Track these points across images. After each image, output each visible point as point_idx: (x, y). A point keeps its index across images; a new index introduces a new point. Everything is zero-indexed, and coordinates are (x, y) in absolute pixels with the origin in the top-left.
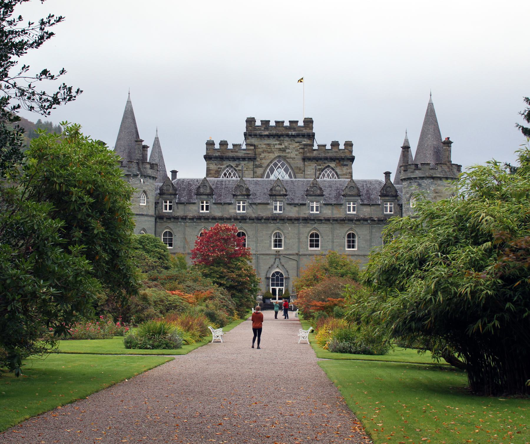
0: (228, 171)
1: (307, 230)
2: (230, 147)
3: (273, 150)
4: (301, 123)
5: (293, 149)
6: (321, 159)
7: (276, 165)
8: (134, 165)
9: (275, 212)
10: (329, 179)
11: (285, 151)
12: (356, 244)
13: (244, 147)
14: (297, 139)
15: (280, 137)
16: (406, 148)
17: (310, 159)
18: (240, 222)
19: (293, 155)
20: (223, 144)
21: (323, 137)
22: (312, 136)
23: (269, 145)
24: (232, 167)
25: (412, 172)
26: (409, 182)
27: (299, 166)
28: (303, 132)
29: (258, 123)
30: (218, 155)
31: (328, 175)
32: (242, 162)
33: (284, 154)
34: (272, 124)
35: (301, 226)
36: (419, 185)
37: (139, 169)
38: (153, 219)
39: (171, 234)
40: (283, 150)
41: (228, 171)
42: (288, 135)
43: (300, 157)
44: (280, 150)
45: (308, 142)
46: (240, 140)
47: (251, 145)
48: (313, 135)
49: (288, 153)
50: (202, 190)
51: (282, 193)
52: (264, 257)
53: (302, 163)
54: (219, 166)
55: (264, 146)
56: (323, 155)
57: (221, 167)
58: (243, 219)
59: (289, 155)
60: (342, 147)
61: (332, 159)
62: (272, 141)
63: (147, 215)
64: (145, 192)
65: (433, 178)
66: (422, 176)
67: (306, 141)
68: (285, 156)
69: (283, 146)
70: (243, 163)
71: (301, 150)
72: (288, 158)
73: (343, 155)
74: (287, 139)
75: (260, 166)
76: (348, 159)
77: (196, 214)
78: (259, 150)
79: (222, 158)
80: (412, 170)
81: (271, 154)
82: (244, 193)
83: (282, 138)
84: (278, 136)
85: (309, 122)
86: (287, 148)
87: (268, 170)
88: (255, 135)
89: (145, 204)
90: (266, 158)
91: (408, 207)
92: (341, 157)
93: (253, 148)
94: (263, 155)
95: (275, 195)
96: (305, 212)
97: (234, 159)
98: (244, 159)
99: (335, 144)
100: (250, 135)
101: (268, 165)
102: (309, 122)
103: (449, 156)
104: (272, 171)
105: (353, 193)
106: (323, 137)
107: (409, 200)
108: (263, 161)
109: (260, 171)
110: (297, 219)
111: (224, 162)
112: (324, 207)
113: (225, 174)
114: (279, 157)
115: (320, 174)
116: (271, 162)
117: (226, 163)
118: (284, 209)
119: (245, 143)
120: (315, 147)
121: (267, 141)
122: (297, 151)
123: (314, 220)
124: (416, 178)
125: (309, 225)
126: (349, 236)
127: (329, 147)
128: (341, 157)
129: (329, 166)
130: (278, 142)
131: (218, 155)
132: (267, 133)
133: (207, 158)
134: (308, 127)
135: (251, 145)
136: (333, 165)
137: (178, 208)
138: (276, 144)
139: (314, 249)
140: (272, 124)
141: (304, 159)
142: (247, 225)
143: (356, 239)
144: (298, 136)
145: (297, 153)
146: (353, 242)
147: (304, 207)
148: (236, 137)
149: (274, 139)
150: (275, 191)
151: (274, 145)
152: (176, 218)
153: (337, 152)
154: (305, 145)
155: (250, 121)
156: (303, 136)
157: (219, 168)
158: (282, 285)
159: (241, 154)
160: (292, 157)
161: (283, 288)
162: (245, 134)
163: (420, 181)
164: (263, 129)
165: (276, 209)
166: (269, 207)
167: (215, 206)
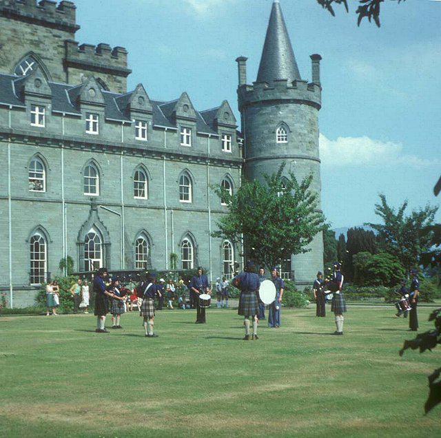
5: (50, 44)
14: (56, 32)
16: (241, 60)
18: (37, 144)
23: (14, 31)
33: (36, 51)
40: (37, 43)
44: (32, 42)
55: (9, 32)
58: (41, 140)
59: (44, 54)
62: (23, 28)
67: (65, 36)
68: (39, 54)
69: (36, 38)
71: (61, 50)
107: (274, 132)
122: (55, 48)
124: (288, 101)
136: (104, 77)
138: (26, 33)
141: (67, 64)
142: (47, 149)
145: (56, 52)
154: (66, 42)
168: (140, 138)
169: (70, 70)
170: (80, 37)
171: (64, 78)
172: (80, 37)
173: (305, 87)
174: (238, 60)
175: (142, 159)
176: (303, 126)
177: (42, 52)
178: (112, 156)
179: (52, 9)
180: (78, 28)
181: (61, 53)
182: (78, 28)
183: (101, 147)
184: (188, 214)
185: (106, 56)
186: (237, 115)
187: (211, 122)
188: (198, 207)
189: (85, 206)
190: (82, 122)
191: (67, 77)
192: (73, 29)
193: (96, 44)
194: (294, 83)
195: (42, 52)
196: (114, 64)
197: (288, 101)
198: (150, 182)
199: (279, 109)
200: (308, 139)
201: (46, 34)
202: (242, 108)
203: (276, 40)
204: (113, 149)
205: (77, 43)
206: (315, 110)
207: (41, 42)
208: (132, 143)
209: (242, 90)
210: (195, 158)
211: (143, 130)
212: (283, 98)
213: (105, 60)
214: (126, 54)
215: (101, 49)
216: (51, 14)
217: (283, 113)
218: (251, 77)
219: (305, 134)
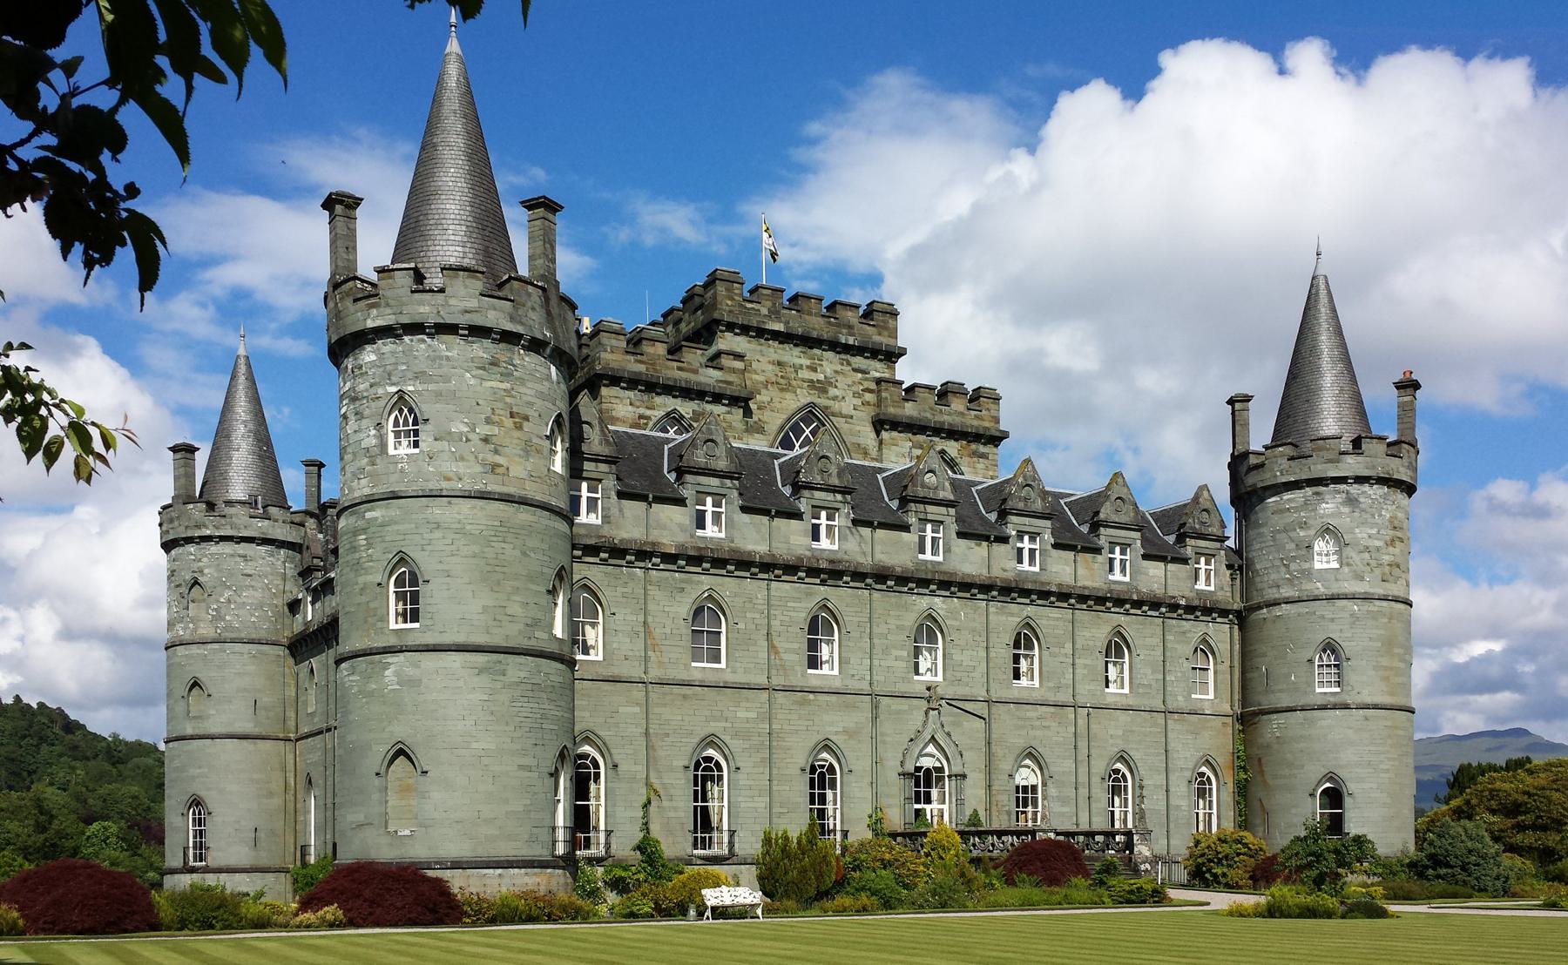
3: (794, 383)
5: (847, 390)
11: (823, 391)
14: (858, 361)
16: (1238, 402)
19: (846, 407)
25: (1330, 461)
26: (1309, 491)
27: (862, 441)
32: (709, 407)
33: (822, 401)
35: (994, 607)
36: (1351, 501)
40: (821, 387)
44: (812, 384)
49: (835, 398)
51: (942, 495)
52: (896, 704)
53: (873, 435)
54: (642, 411)
55: (770, 367)
57: (648, 413)
58: (833, 573)
59: (836, 406)
62: (793, 355)
67: (877, 369)
69: (821, 377)
71: (869, 397)
74: (830, 354)
77: (682, 538)
78: (755, 377)
81: (788, 395)
82: (835, 481)
83: (817, 351)
84: (807, 342)
86: (830, 384)
88: (745, 330)
91: (1306, 566)
95: (925, 501)
105: (1123, 519)
111: (659, 400)
112: (1055, 553)
117: (665, 404)
118: (947, 550)
121: (775, 351)
124: (1342, 480)
130: (808, 362)
132: (778, 327)
134: (886, 328)
136: (952, 448)
137: (621, 510)
138: (801, 367)
141: (879, 424)
144: (859, 350)
145: (858, 402)
149: (797, 351)
150: (923, 486)
151: (797, 368)
152: (618, 552)
154: (879, 381)
157: (641, 417)
160: (845, 412)
163: (1355, 489)
167: (746, 518)
168: (1026, 566)
169: (885, 435)
170: (905, 371)
171: (874, 453)
172: (905, 371)
173: (1381, 448)
174: (1231, 402)
175: (1029, 608)
176: (1374, 531)
177: (830, 403)
178: (969, 603)
179: (852, 317)
180: (902, 352)
181: (868, 403)
182: (902, 352)
185: (958, 405)
186: (1230, 515)
187: (1172, 533)
189: (915, 702)
190: (910, 538)
191: (880, 449)
192: (892, 355)
193: (938, 383)
194: (1357, 443)
195: (830, 403)
196: (971, 421)
197: (1342, 480)
198: (1045, 653)
199: (1323, 501)
200: (1386, 559)
201: (839, 368)
202: (1236, 500)
203: (1314, 351)
205: (901, 383)
206: (1400, 497)
207: (830, 384)
208: (1010, 575)
209: (1239, 463)
210: (1137, 604)
211: (1032, 551)
212: (370, 324)
213: (956, 412)
214: (997, 399)
215: (945, 393)
216: (850, 327)
217: (1330, 505)
218: (1260, 435)
219: (1378, 549)
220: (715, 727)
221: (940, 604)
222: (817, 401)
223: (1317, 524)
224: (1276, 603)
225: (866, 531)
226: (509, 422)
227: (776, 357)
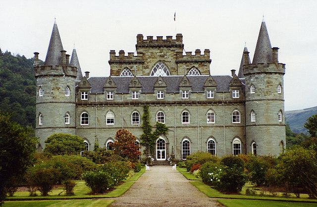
0: (125, 71)
1: (179, 110)
2: (126, 54)
4: (174, 38)
5: (169, 55)
6: (188, 62)
7: (158, 66)
8: (60, 68)
9: (158, 98)
10: (195, 76)
12: (189, 119)
13: (136, 54)
15: (160, 48)
16: (246, 53)
17: (181, 62)
18: (135, 106)
19: (169, 60)
20: (122, 52)
21: (190, 46)
22: (182, 47)
24: (128, 68)
28: (174, 44)
29: (145, 38)
30: (118, 60)
31: (194, 73)
33: (163, 59)
34: (155, 38)
37: (64, 72)
38: (75, 105)
39: (87, 115)
40: (163, 56)
41: (125, 71)
42: (165, 46)
43: (174, 60)
45: (180, 51)
46: (133, 50)
47: (141, 53)
48: (183, 46)
50: (108, 85)
56: (190, 59)
59: (166, 60)
60: (202, 53)
61: (196, 62)
63: (70, 103)
64: (68, 86)
65: (266, 73)
66: (258, 72)
68: (164, 60)
70: (135, 66)
72: (166, 62)
73: (203, 59)
74: (165, 48)
75: (147, 67)
76: (207, 61)
79: (121, 63)
80: (251, 68)
84: (159, 47)
85: (179, 37)
87: (153, 70)
89: (69, 95)
90: (151, 63)
92: (202, 60)
93: (142, 55)
94: (149, 60)
96: (178, 98)
97: (129, 63)
98: (136, 63)
99: (198, 52)
100: (140, 47)
101: (153, 67)
102: (179, 37)
103: (277, 58)
104: (155, 70)
106: (190, 46)
107: (250, 89)
108: (149, 64)
109: (147, 71)
110: (174, 103)
112: (192, 94)
113: (123, 74)
114: (160, 61)
115: (188, 72)
116: (155, 65)
117: (124, 66)
119: (136, 52)
120: (184, 54)
123: (185, 103)
124: (254, 73)
125: (182, 107)
126: (184, 114)
127: (193, 54)
128: (202, 60)
129: (194, 67)
131: (118, 60)
133: (110, 63)
135: (141, 53)
136: (196, 65)
139: (185, 123)
140: (155, 38)
141: (177, 63)
143: (189, 116)
144: (172, 46)
146: (187, 117)
147: (178, 95)
148: (130, 47)
153: (199, 57)
154: (177, 52)
155: (140, 37)
156: (176, 46)
158: (164, 148)
159: (133, 59)
161: (165, 150)
162: (136, 46)
163: (256, 76)
164: (148, 42)
165: (159, 97)
166: (154, 95)
167: (117, 95)
170: (187, 49)
183: (163, 103)
184: (212, 129)
188: (219, 125)
204: (170, 104)
220: (111, 136)
221: (162, 108)
222: (161, 59)
223: (250, 83)
224: (253, 100)
225: (144, 95)
226: (56, 89)
227: (150, 51)
